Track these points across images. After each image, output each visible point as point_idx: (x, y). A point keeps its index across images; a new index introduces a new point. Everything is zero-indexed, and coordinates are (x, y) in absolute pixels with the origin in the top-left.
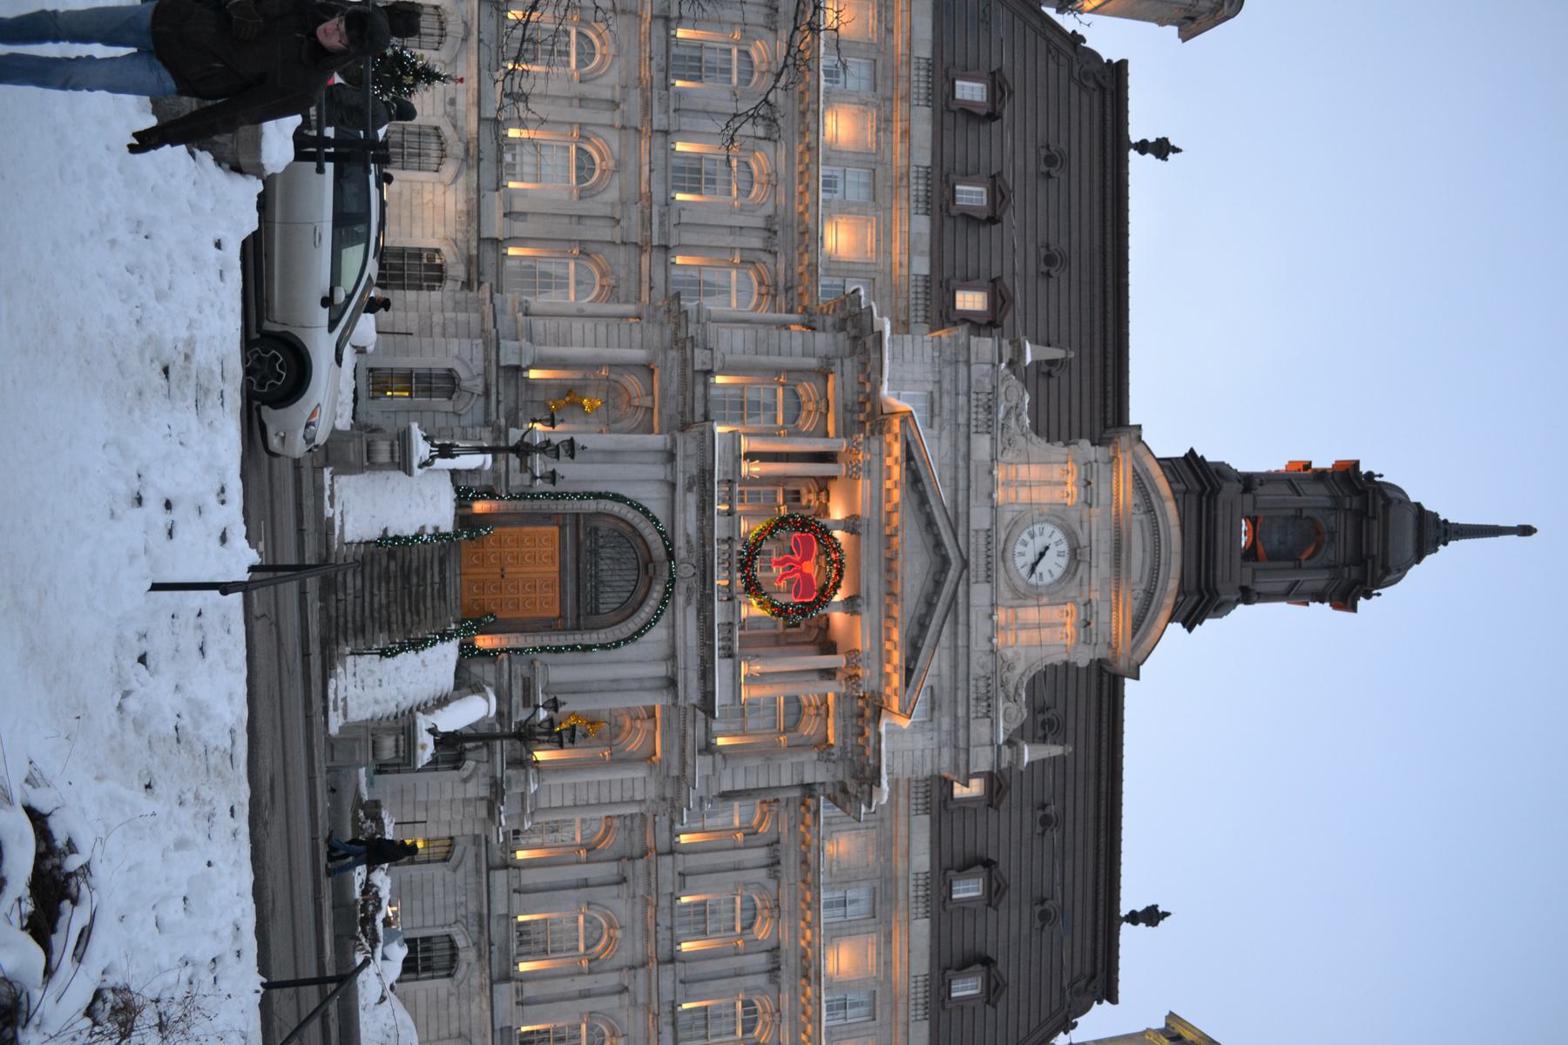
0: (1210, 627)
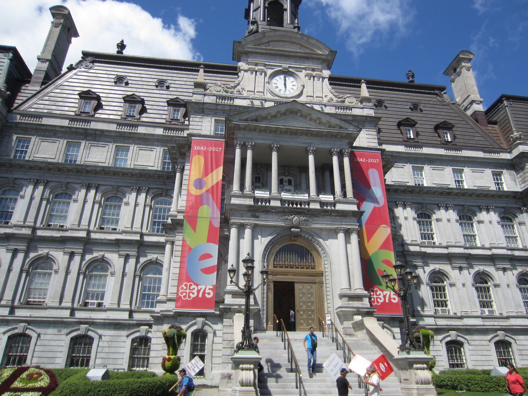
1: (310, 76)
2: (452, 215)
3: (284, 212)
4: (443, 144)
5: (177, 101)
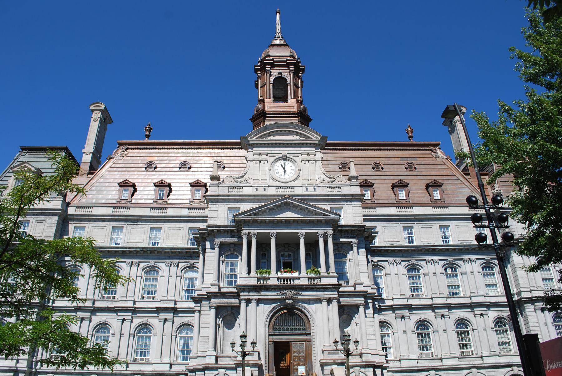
0: (309, 113)
1: (305, 161)
2: (439, 268)
5: (198, 183)
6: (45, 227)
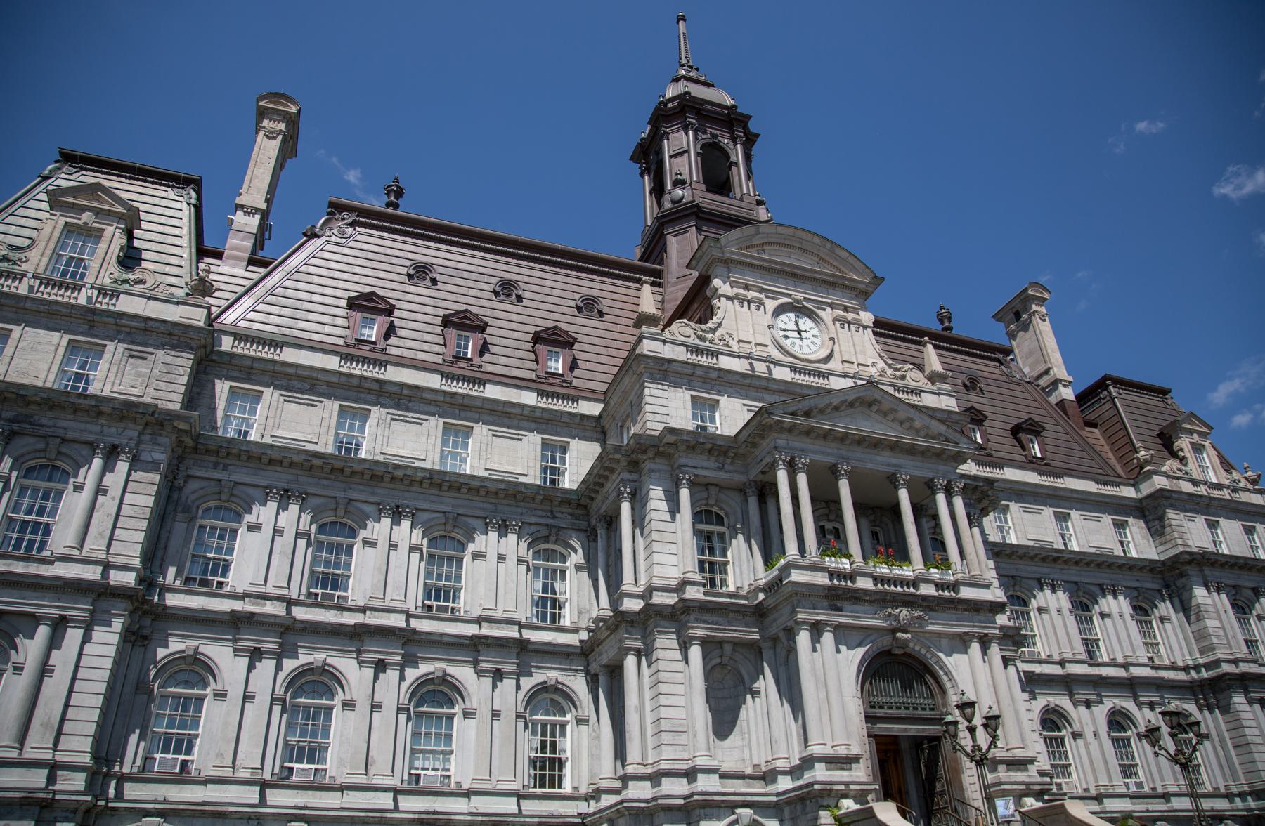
3: (884, 601)
4: (1030, 462)
5: (556, 334)
6: (156, 371)
